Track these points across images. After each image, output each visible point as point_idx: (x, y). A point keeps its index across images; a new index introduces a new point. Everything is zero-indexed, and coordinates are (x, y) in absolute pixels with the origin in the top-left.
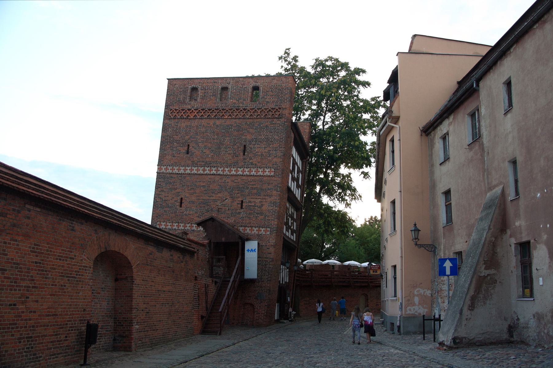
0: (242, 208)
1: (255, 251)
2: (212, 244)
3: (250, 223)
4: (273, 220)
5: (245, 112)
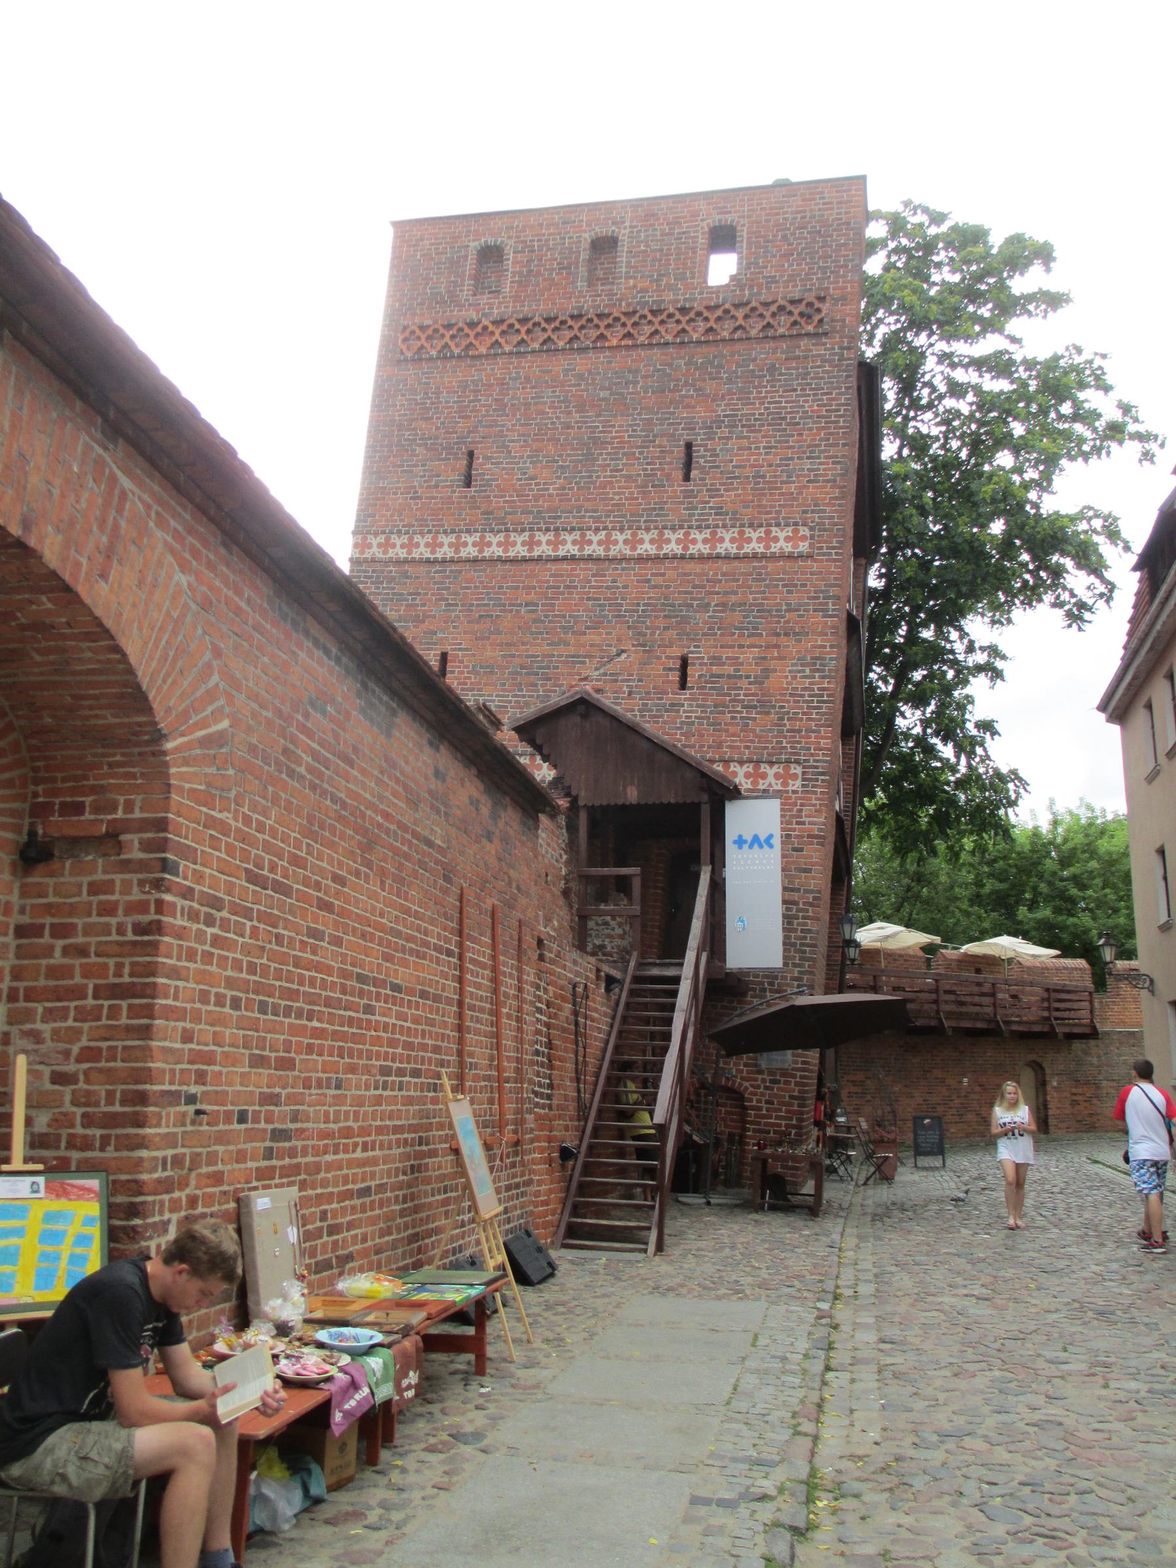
0: (683, 685)
1: (771, 846)
2: (583, 817)
3: (720, 746)
4: (814, 731)
5: (684, 319)
